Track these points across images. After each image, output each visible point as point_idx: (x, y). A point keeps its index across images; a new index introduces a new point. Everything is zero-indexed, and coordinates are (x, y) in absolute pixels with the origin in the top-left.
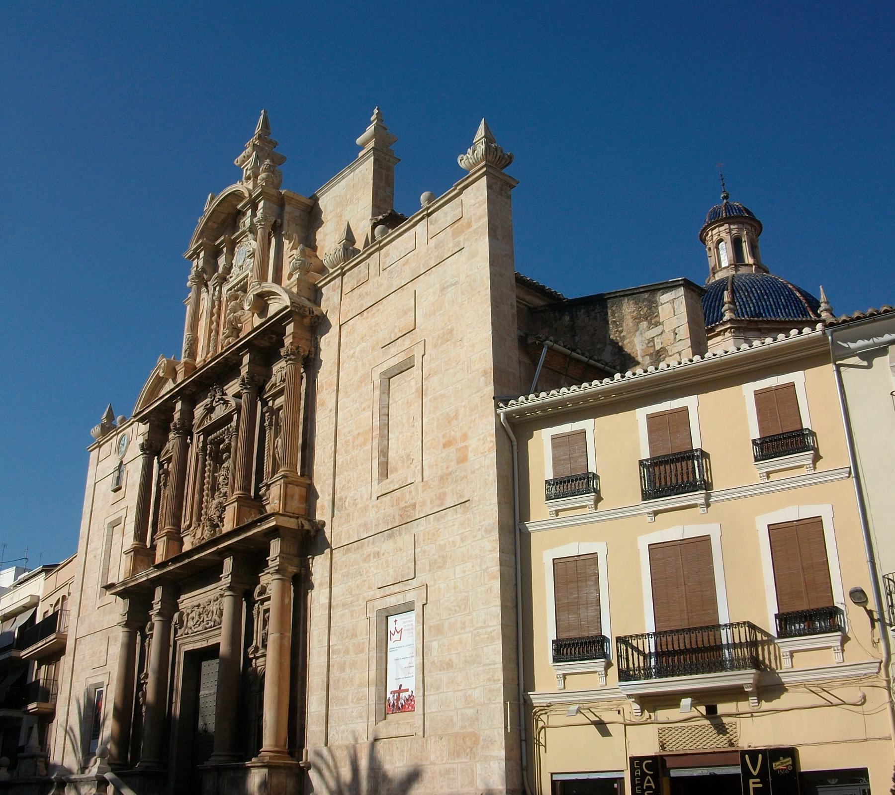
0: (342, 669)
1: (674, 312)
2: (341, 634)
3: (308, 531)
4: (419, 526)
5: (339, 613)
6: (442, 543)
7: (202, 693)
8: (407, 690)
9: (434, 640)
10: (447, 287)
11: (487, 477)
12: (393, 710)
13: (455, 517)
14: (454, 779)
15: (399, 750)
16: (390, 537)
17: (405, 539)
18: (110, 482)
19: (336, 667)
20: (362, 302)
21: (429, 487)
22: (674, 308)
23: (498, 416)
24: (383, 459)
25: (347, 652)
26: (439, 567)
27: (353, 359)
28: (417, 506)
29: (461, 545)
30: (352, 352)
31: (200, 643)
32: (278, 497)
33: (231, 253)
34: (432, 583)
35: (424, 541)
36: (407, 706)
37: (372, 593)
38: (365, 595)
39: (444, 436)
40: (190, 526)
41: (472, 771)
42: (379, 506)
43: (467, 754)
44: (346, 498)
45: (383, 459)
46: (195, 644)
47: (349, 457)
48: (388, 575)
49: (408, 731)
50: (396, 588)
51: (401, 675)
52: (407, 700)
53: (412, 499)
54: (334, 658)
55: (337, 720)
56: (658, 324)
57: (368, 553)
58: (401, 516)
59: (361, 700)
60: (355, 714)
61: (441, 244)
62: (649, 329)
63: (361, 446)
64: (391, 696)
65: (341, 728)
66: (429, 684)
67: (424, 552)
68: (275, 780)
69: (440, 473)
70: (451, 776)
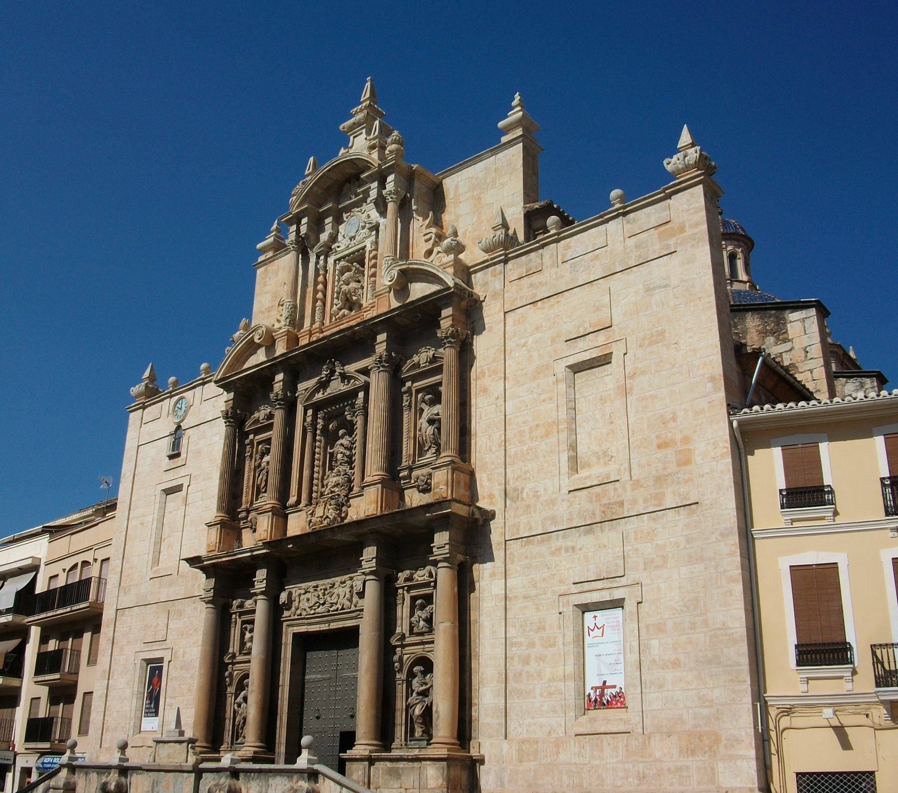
0: (526, 661)
1: (805, 331)
2: (522, 626)
3: (477, 520)
4: (628, 524)
5: (520, 605)
6: (659, 542)
8: (614, 687)
9: (654, 639)
10: (654, 288)
11: (720, 481)
12: (595, 706)
13: (677, 518)
14: (688, 777)
15: (612, 746)
16: (587, 533)
17: (610, 536)
18: (165, 446)
19: (516, 659)
20: (534, 291)
21: (641, 486)
22: (804, 327)
23: (731, 423)
24: (572, 453)
25: (532, 645)
26: (658, 567)
27: (525, 348)
28: (625, 504)
29: (687, 547)
30: (523, 341)
31: (318, 626)
32: (444, 482)
33: (338, 221)
34: (649, 582)
35: (635, 539)
36: (614, 702)
37: (566, 587)
38: (556, 589)
39: (657, 437)
40: (298, 502)
41: (712, 768)
42: (571, 500)
43: (705, 753)
44: (523, 489)
45: (572, 453)
46: (309, 627)
47: (525, 448)
48: (588, 570)
49: (622, 728)
50: (599, 585)
51: (604, 670)
52: (615, 696)
53: (618, 496)
54: (513, 651)
55: (520, 713)
56: (786, 340)
57: (558, 547)
58: (604, 512)
59: (554, 694)
60: (545, 708)
61: (644, 245)
62: (776, 344)
63: (542, 438)
64: (592, 692)
65: (526, 722)
66: (648, 682)
67: (637, 550)
68: (452, 773)
69: (654, 473)
70: (685, 774)
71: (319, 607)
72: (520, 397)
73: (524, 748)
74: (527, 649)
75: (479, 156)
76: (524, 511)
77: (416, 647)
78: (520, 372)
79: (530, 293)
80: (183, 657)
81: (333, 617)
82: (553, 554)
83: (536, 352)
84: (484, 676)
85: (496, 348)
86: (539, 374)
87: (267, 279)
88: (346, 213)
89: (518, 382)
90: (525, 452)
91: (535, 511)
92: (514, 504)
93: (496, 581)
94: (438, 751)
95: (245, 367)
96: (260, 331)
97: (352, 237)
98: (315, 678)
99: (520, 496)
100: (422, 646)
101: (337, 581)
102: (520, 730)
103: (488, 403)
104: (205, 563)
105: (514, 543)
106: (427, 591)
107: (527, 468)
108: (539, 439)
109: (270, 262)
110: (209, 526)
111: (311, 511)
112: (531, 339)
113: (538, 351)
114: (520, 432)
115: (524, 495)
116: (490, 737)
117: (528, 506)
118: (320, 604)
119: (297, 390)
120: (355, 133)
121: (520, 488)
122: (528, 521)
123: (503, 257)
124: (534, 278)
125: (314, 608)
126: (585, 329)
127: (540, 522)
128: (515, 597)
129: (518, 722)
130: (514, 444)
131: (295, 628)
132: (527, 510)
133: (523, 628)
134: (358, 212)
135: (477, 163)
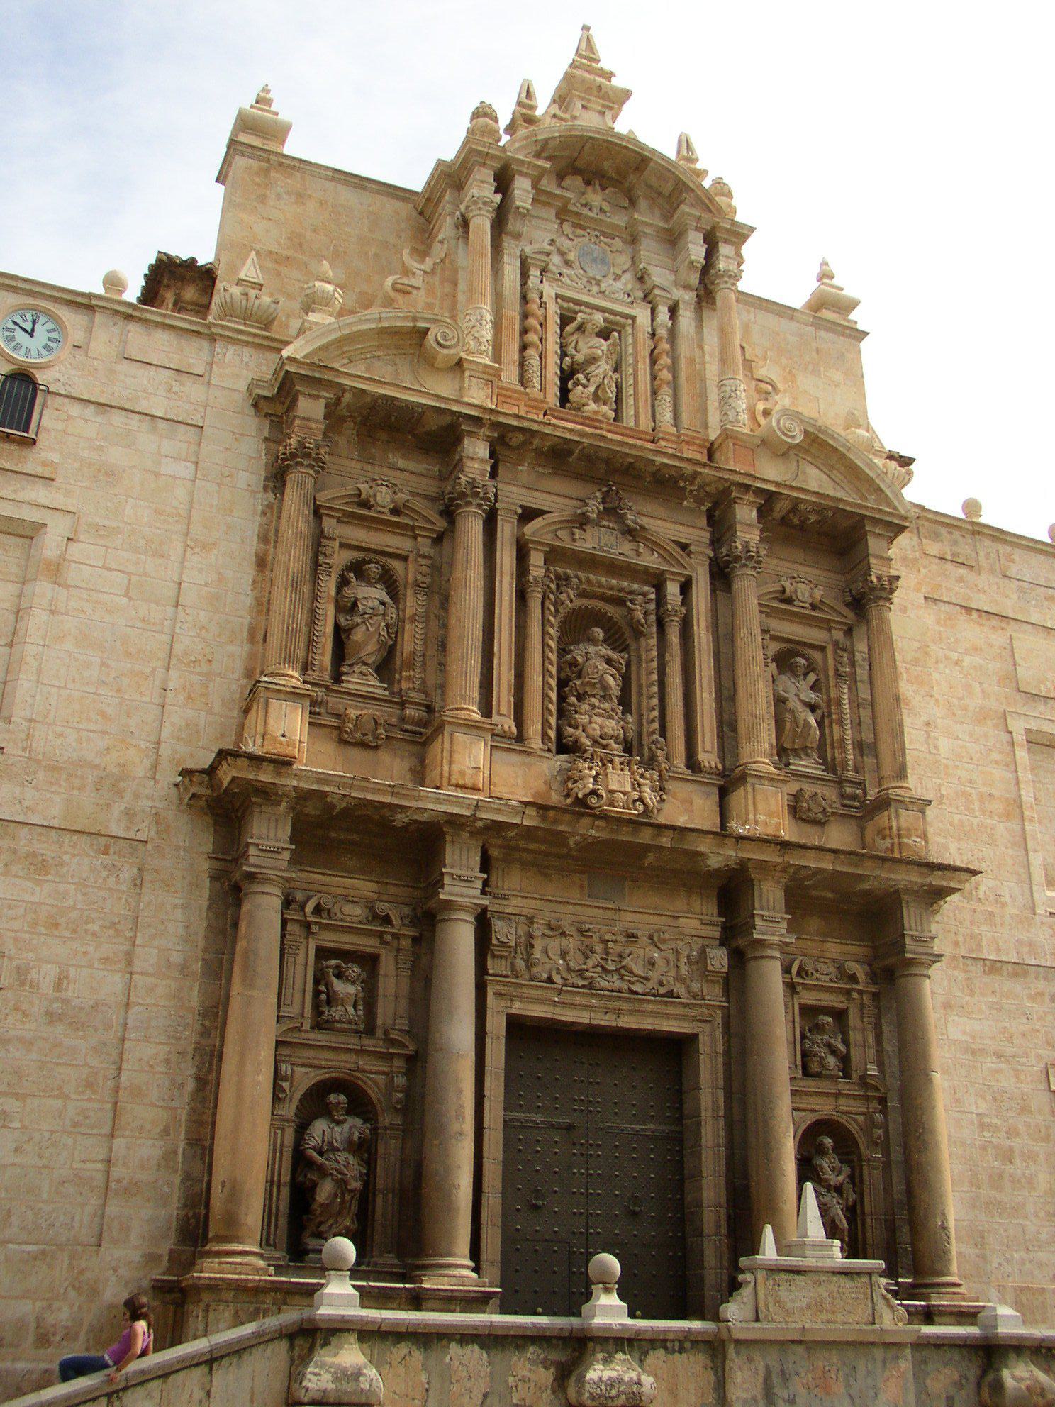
25: (1012, 1132)
30: (955, 656)
46: (558, 1011)
47: (976, 822)
60: (1044, 1236)
63: (999, 817)
72: (958, 738)
73: (1024, 1300)
80: (58, 985)
82: (1033, 998)
89: (954, 714)
91: (1002, 925)
98: (527, 1121)
102: (1008, 1268)
108: (996, 818)
112: (967, 661)
114: (964, 792)
117: (992, 914)
124: (963, 571)
126: (1048, 691)
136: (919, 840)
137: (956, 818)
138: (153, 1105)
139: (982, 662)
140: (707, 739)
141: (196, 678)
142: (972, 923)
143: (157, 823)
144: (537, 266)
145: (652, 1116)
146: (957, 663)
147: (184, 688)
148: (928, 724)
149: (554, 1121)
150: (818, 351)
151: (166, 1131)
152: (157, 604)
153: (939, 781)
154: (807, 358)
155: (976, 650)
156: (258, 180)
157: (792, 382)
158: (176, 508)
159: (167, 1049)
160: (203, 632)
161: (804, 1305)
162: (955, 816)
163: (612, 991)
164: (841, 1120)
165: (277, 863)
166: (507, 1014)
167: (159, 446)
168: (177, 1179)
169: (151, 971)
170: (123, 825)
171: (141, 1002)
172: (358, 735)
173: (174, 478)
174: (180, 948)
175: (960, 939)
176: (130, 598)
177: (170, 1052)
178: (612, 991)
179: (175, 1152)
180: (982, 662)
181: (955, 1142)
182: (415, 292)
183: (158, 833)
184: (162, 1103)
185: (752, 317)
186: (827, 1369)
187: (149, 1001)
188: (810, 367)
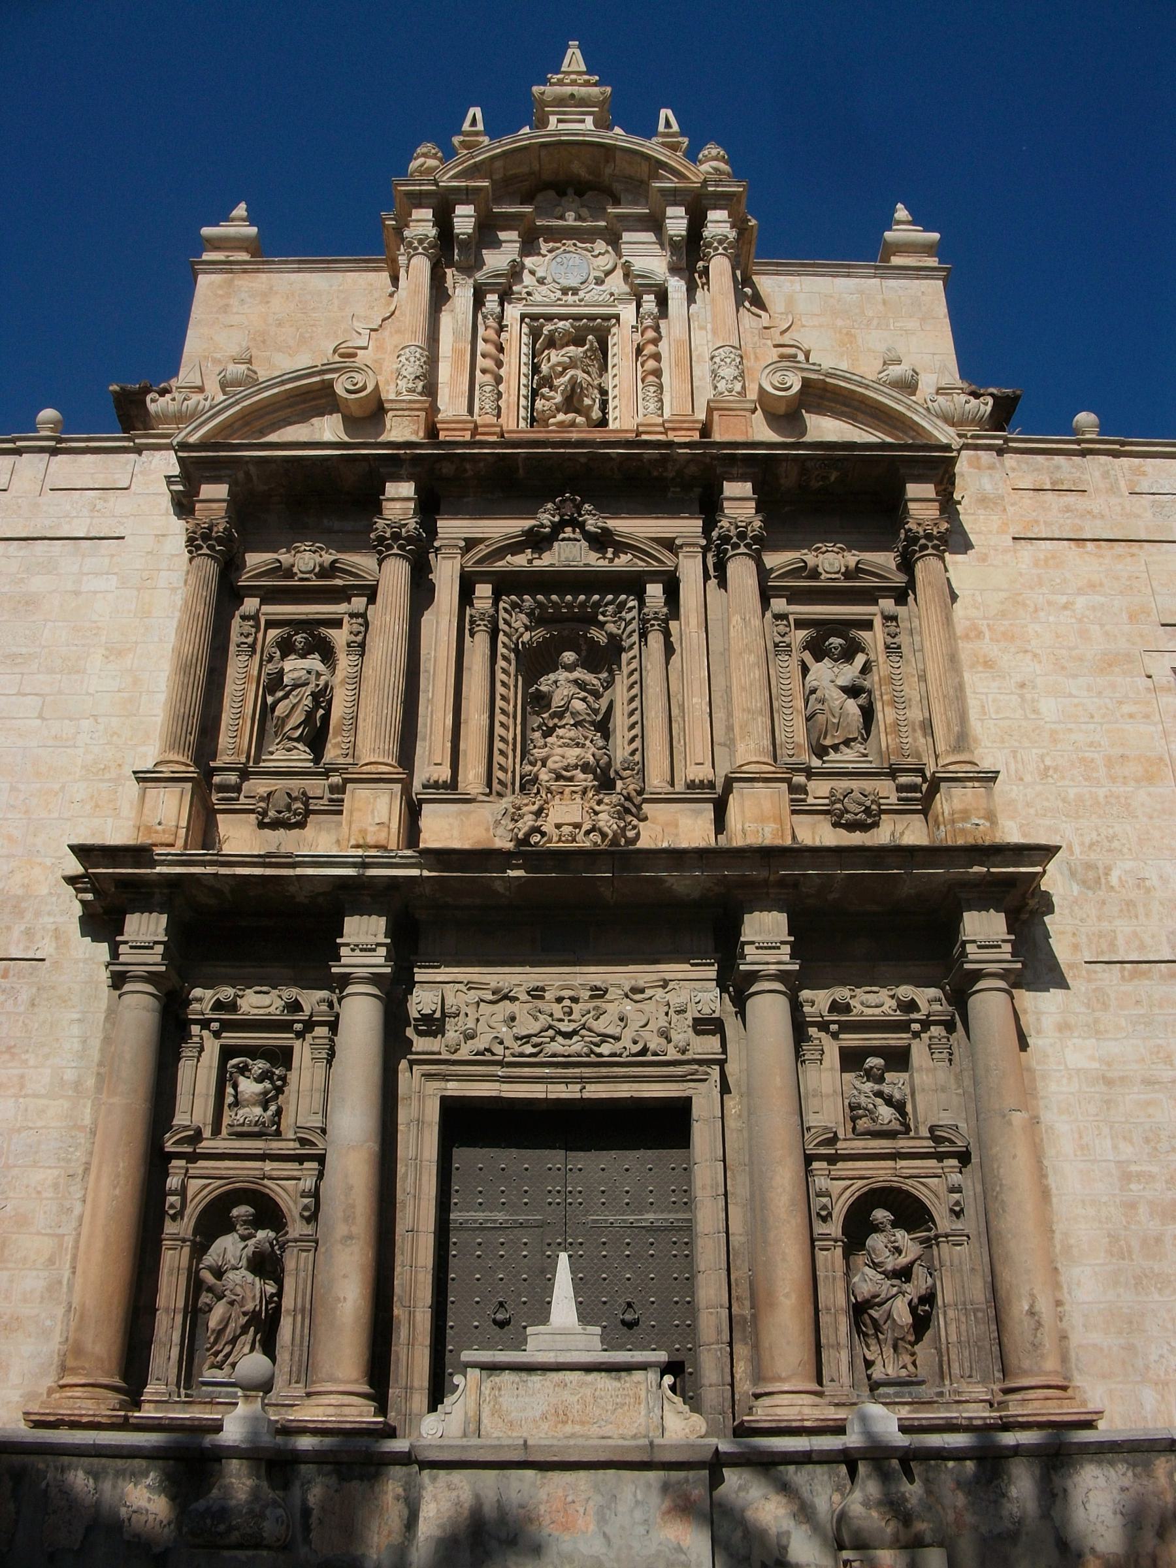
7: (452, 1216)
31: (541, 1087)
33: (529, 246)
46: (505, 1087)
47: (1101, 793)
63: (1137, 781)
71: (553, 1039)
72: (1071, 695)
74: (1170, 1189)
75: (849, 266)
76: (1121, 911)
77: (870, 1164)
78: (1064, 652)
79: (1069, 521)
81: (604, 1071)
83: (1097, 627)
84: (1072, 1241)
85: (1003, 595)
86: (1110, 665)
87: (234, 301)
88: (546, 241)
89: (1063, 668)
90: (1101, 799)
92: (1090, 893)
93: (1075, 1041)
94: (1060, 1407)
95: (273, 438)
96: (359, 378)
97: (571, 289)
99: (1103, 881)
100: (890, 1163)
101: (619, 986)
103: (999, 688)
104: (158, 870)
105: (1104, 971)
106: (894, 1039)
107: (1111, 831)
108: (1132, 783)
109: (245, 271)
110: (139, 780)
111: (536, 807)
112: (1081, 602)
113: (1102, 625)
114: (1082, 760)
115: (1114, 880)
116: (1104, 1377)
117: (1130, 904)
118: (560, 1033)
119: (437, 533)
120: (565, 113)
121: (1100, 864)
122: (1135, 934)
123: (1001, 442)
124: (1070, 499)
125: (535, 1040)
127: (1164, 939)
128: (1122, 1079)
129: (1169, 1343)
130: (1073, 780)
131: (451, 1085)
132: (1128, 910)
133: (1152, 1144)
134: (587, 250)
135: (838, 276)
136: (981, 822)
137: (1072, 793)
138: (39, 1233)
139: (1102, 599)
140: (699, 748)
141: (104, 786)
142: (1099, 919)
143: (57, 938)
144: (492, 292)
145: (652, 1204)
146: (1065, 607)
147: (92, 797)
148: (1022, 685)
149: (521, 1218)
150: (884, 302)
151: (51, 1261)
152: (71, 719)
153: (1040, 751)
154: (871, 314)
155: (1092, 586)
156: (220, 292)
157: (851, 343)
158: (95, 622)
159: (56, 1172)
160: (115, 738)
161: (538, 1415)
162: (1069, 790)
163: (569, 1056)
164: (905, 1187)
165: (150, 959)
166: (444, 1099)
167: (81, 566)
168: (60, 1311)
169: (43, 1091)
170: (21, 946)
171: (30, 1125)
172: (272, 813)
173: (95, 593)
174: (74, 1065)
175: (1083, 940)
176: (43, 719)
177: (59, 1176)
178: (569, 1056)
179: (60, 1282)
180: (1102, 599)
181: (1083, 1201)
182: (359, 352)
183: (57, 948)
184: (49, 1231)
185: (797, 287)
186: (570, 1499)
187: (40, 1124)
188: (875, 322)
